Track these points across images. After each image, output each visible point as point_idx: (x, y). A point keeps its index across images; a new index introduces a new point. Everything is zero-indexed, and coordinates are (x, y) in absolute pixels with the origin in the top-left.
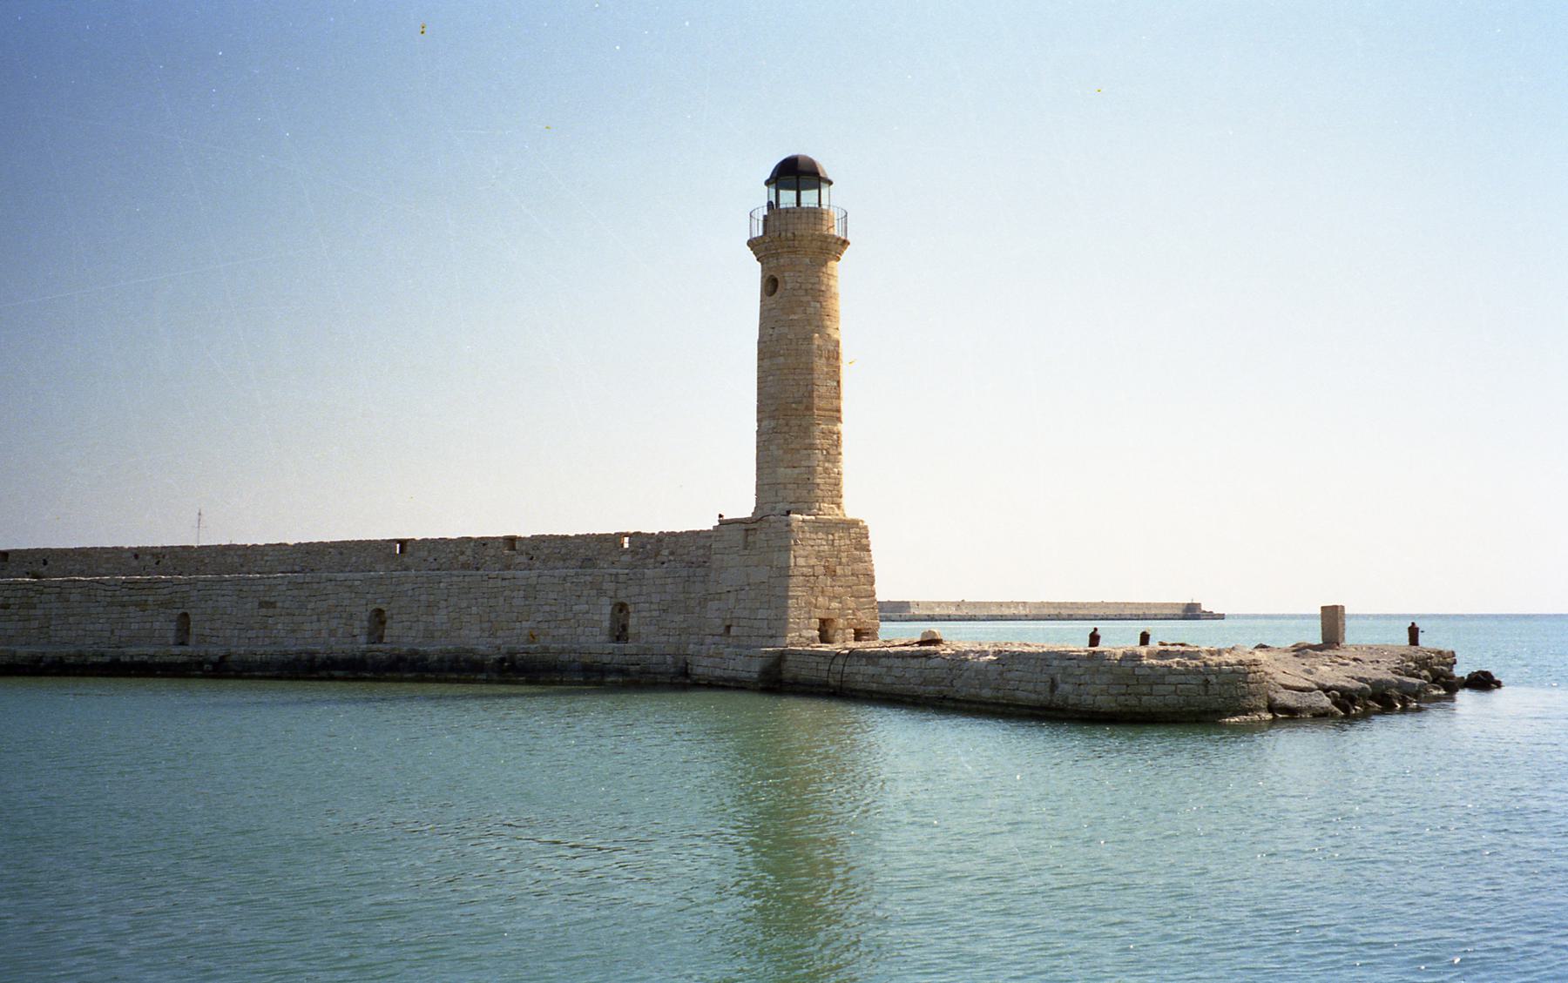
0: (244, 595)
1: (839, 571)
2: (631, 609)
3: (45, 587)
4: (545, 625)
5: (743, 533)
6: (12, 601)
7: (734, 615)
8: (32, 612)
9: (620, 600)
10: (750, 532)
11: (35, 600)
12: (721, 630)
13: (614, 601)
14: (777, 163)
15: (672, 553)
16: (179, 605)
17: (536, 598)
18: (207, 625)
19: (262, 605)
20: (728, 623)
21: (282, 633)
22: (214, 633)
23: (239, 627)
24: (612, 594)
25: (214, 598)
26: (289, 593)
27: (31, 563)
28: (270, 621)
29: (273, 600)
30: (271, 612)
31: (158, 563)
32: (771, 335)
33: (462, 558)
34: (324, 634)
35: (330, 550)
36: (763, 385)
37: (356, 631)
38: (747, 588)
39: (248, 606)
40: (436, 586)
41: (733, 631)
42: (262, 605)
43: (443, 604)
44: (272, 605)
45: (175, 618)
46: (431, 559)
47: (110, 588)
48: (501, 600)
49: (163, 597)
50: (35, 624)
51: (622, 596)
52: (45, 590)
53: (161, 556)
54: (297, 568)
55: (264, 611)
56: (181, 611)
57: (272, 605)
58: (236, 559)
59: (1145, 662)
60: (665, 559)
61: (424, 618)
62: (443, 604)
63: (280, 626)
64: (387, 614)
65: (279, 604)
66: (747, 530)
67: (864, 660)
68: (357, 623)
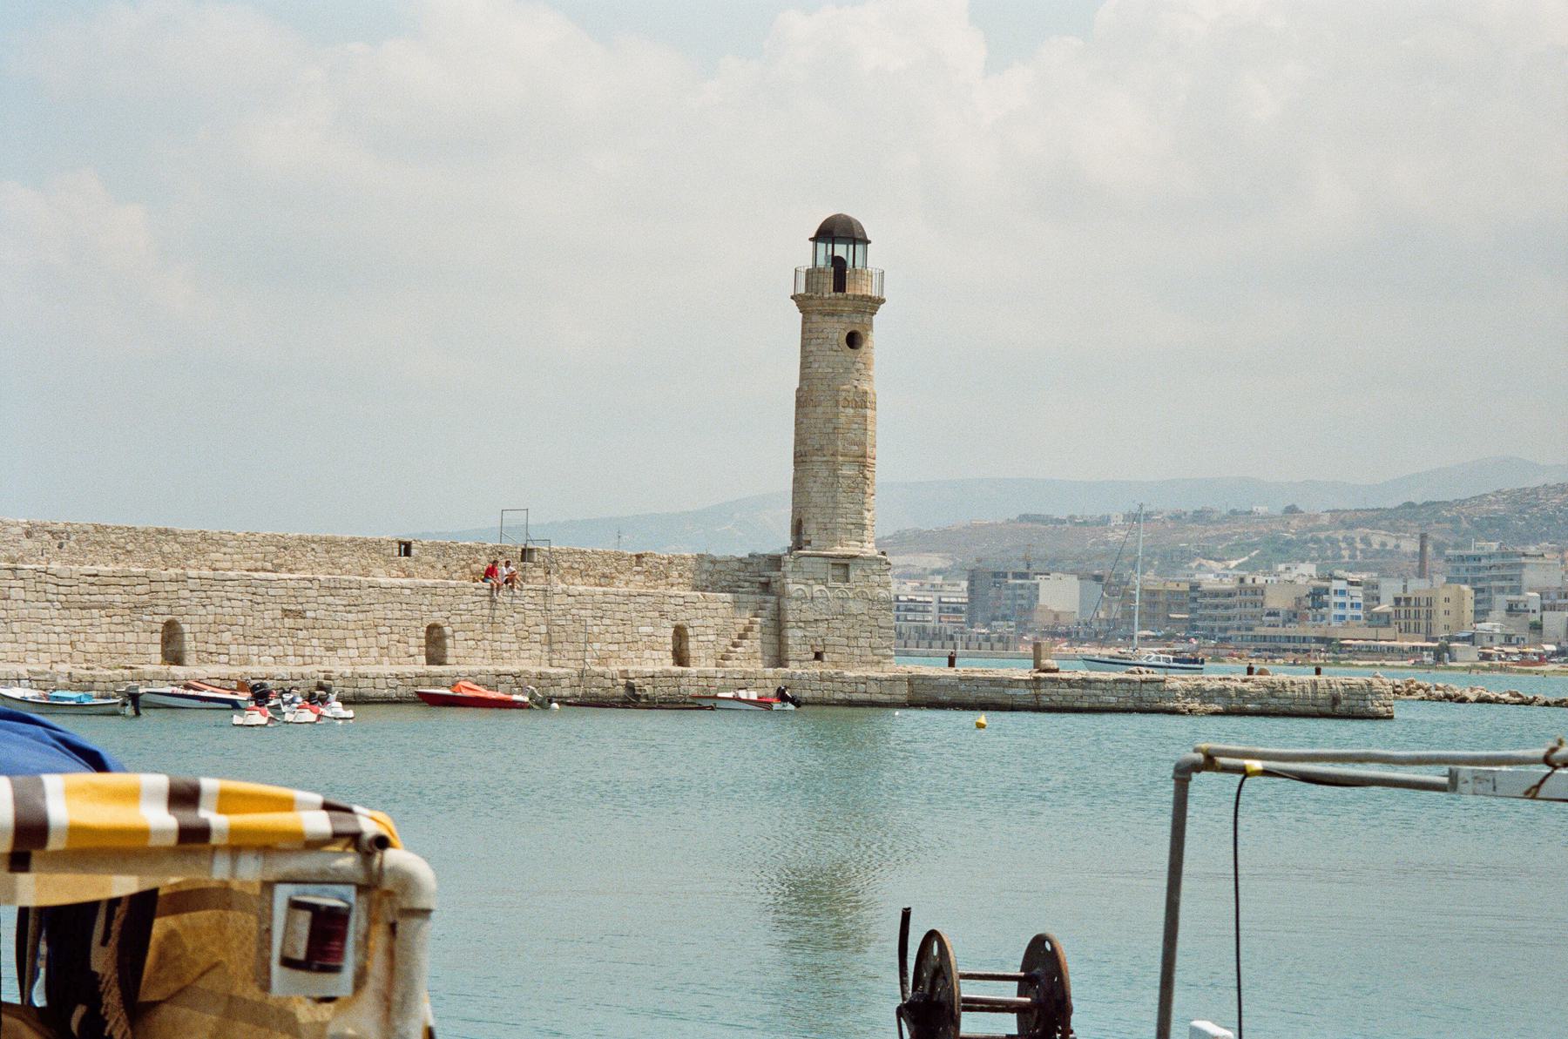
0: (260, 599)
2: (690, 632)
7: (826, 642)
12: (812, 655)
15: (681, 576)
16: (164, 609)
17: (602, 618)
18: (212, 638)
19: (287, 613)
20: (819, 649)
23: (256, 641)
25: (216, 601)
30: (301, 622)
31: (60, 546)
32: (856, 387)
35: (314, 546)
37: (413, 650)
42: (287, 613)
43: (508, 620)
44: (300, 614)
45: (160, 627)
46: (440, 566)
47: (67, 582)
49: (134, 598)
51: (682, 618)
54: (269, 566)
55: (289, 622)
57: (300, 614)
64: (448, 630)
65: (309, 614)
68: (412, 641)
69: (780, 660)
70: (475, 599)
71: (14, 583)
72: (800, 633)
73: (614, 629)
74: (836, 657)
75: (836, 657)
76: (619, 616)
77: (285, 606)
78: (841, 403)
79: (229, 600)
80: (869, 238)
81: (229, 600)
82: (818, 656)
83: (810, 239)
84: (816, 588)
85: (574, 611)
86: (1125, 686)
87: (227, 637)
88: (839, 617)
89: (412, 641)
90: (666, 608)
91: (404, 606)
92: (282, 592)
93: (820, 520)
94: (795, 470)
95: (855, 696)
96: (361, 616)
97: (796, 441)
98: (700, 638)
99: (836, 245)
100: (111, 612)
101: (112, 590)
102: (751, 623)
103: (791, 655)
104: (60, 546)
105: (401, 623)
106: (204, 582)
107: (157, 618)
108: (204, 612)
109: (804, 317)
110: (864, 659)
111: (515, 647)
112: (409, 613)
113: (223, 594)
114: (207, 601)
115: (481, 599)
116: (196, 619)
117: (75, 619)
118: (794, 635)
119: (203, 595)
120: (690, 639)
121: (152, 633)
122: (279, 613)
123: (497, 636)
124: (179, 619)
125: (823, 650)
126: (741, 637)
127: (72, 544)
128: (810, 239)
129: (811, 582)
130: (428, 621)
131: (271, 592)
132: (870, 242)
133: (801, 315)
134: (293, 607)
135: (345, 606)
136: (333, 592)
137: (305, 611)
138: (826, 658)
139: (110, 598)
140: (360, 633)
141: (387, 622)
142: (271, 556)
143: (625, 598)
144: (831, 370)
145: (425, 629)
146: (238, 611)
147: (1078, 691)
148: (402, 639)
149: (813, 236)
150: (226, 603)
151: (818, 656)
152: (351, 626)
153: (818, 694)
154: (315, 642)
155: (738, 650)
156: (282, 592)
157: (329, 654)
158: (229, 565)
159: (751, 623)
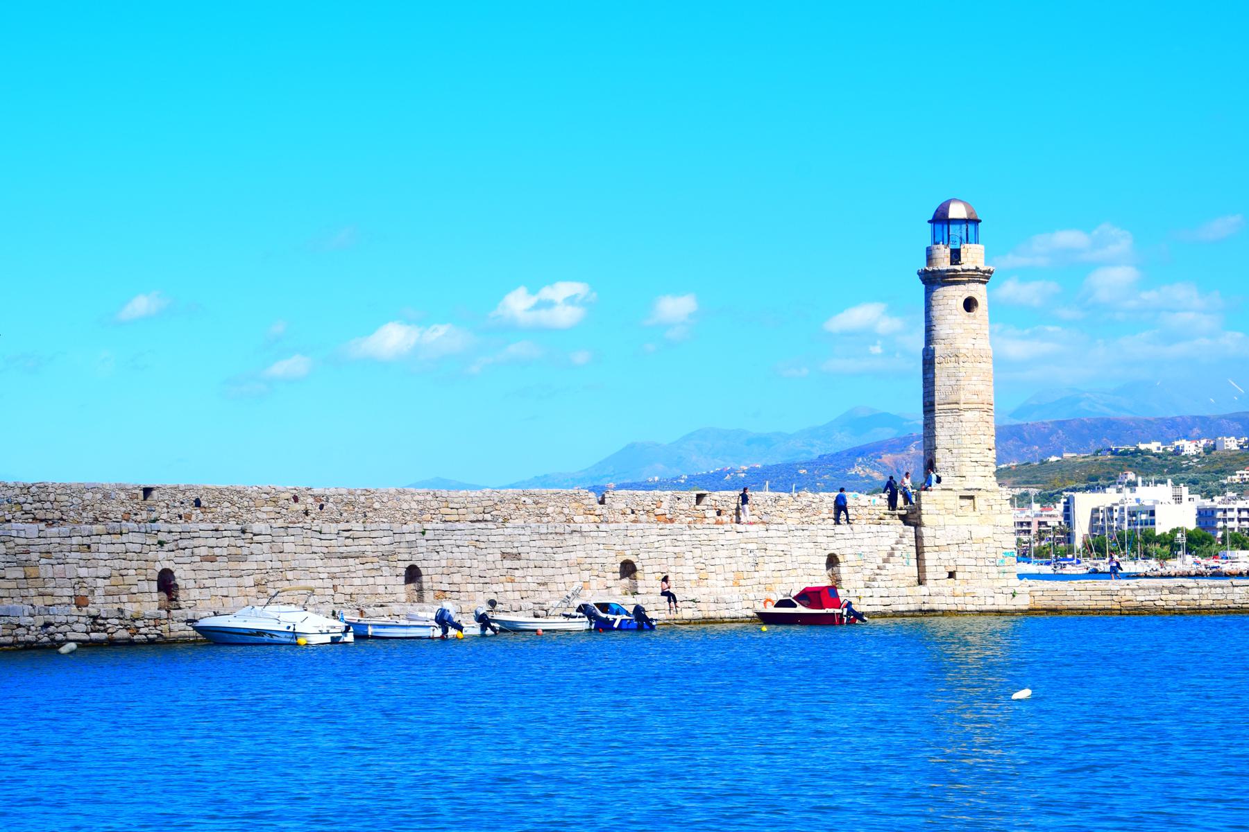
0: (483, 545)
3: (255, 535)
4: (776, 574)
6: (217, 551)
7: (958, 563)
8: (243, 566)
9: (832, 552)
11: (245, 551)
12: (947, 575)
13: (828, 552)
16: (406, 557)
17: (766, 549)
18: (446, 579)
20: (952, 569)
22: (455, 588)
23: (482, 580)
24: (826, 547)
26: (532, 544)
27: (182, 503)
28: (517, 573)
29: (515, 551)
30: (516, 564)
31: (321, 507)
33: (658, 511)
36: (926, 381)
38: (970, 542)
39: (490, 558)
40: (679, 538)
41: (958, 575)
42: (504, 556)
43: (688, 555)
44: (517, 556)
45: (403, 571)
46: (629, 511)
47: (327, 537)
48: (739, 551)
50: (249, 581)
52: (256, 538)
53: (324, 498)
54: (488, 517)
55: (508, 563)
56: (407, 564)
57: (517, 556)
58: (414, 505)
62: (688, 555)
63: (529, 579)
69: (921, 582)
70: (660, 538)
71: (286, 539)
72: (935, 555)
73: (777, 559)
74: (968, 576)
75: (968, 576)
76: (781, 547)
77: (503, 550)
78: (961, 359)
79: (458, 547)
80: (979, 218)
81: (458, 547)
82: (952, 575)
83: (929, 222)
84: (947, 517)
85: (742, 545)
86: (1219, 590)
87: (457, 578)
88: (968, 541)
89: (610, 575)
90: (819, 539)
91: (601, 547)
92: (501, 538)
93: (948, 459)
94: (925, 418)
95: (984, 608)
96: (566, 556)
97: (924, 393)
98: (850, 564)
99: (951, 226)
100: (364, 560)
101: (362, 542)
102: (893, 549)
103: (928, 576)
104: (321, 507)
105: (597, 560)
106: (437, 532)
107: (401, 564)
108: (437, 557)
109: (926, 288)
110: (990, 576)
111: (695, 577)
112: (606, 552)
113: (453, 542)
114: (439, 549)
115: (665, 538)
116: (432, 563)
117: (336, 566)
118: (930, 558)
119: (437, 543)
120: (842, 564)
121: (397, 576)
122: (499, 556)
123: (680, 569)
124: (419, 564)
125: (955, 569)
126: (886, 561)
127: (330, 505)
128: (929, 222)
129: (941, 512)
130: (622, 559)
131: (492, 538)
132: (980, 221)
133: (924, 286)
134: (509, 550)
135: (552, 548)
136: (543, 537)
137: (519, 554)
138: (957, 577)
139: (363, 549)
140: (566, 570)
141: (589, 560)
142: (490, 509)
143: (785, 533)
144: (952, 331)
145: (619, 565)
146: (464, 556)
147: (1178, 597)
148: (601, 574)
149: (931, 218)
150: (455, 550)
151: (952, 575)
152: (558, 565)
153: (954, 608)
154: (529, 579)
155: (883, 572)
156: (501, 538)
157: (541, 588)
158: (456, 518)
159: (893, 549)
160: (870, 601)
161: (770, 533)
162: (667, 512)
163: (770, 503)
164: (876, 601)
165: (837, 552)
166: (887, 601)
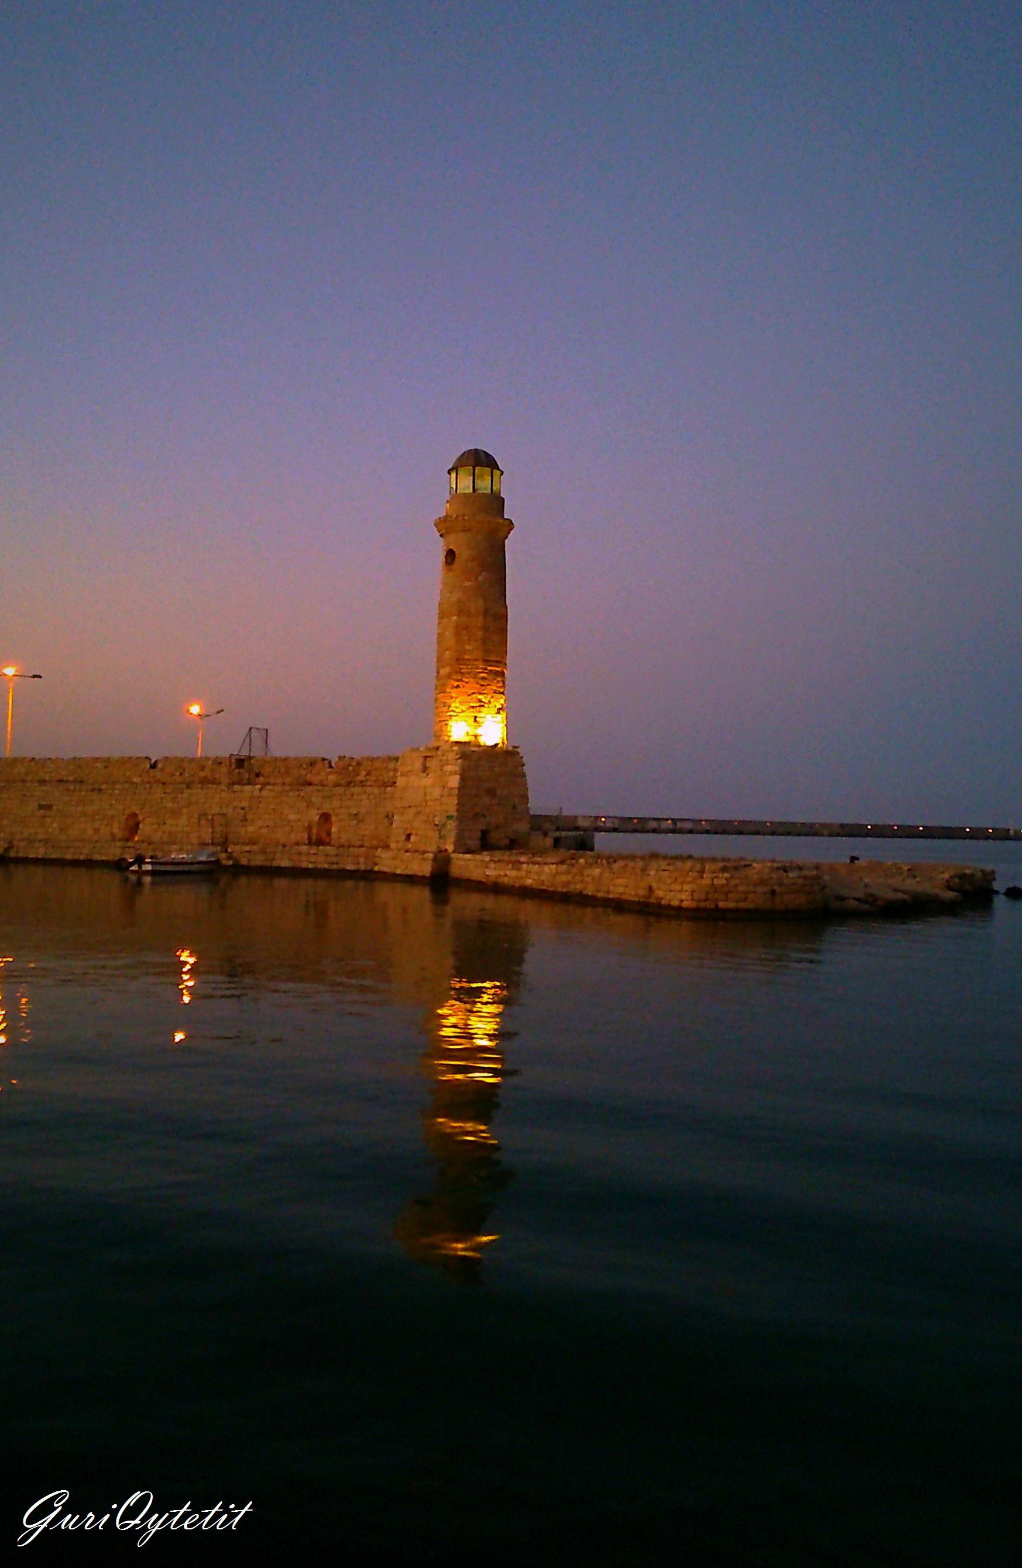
1: (499, 792)
2: (333, 819)
5: (422, 759)
9: (325, 811)
10: (428, 759)
13: (320, 812)
14: (458, 456)
19: (41, 807)
20: (408, 832)
21: (57, 832)
30: (47, 813)
33: (202, 774)
34: (90, 832)
41: (412, 838)
42: (41, 807)
43: (184, 811)
51: (327, 808)
57: (49, 807)
59: (219, 848)
60: (363, 779)
61: (169, 822)
64: (140, 818)
66: (426, 757)
67: (511, 865)
85: (235, 804)
134: (44, 803)
160: (313, 859)
161: (264, 793)
162: (209, 774)
163: (305, 766)
164: (321, 859)
165: (331, 812)
166: (334, 859)
